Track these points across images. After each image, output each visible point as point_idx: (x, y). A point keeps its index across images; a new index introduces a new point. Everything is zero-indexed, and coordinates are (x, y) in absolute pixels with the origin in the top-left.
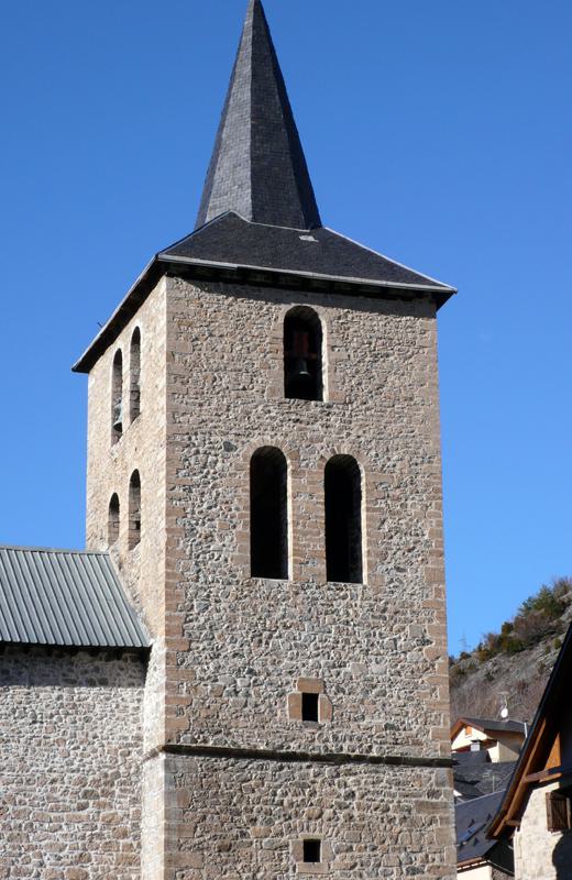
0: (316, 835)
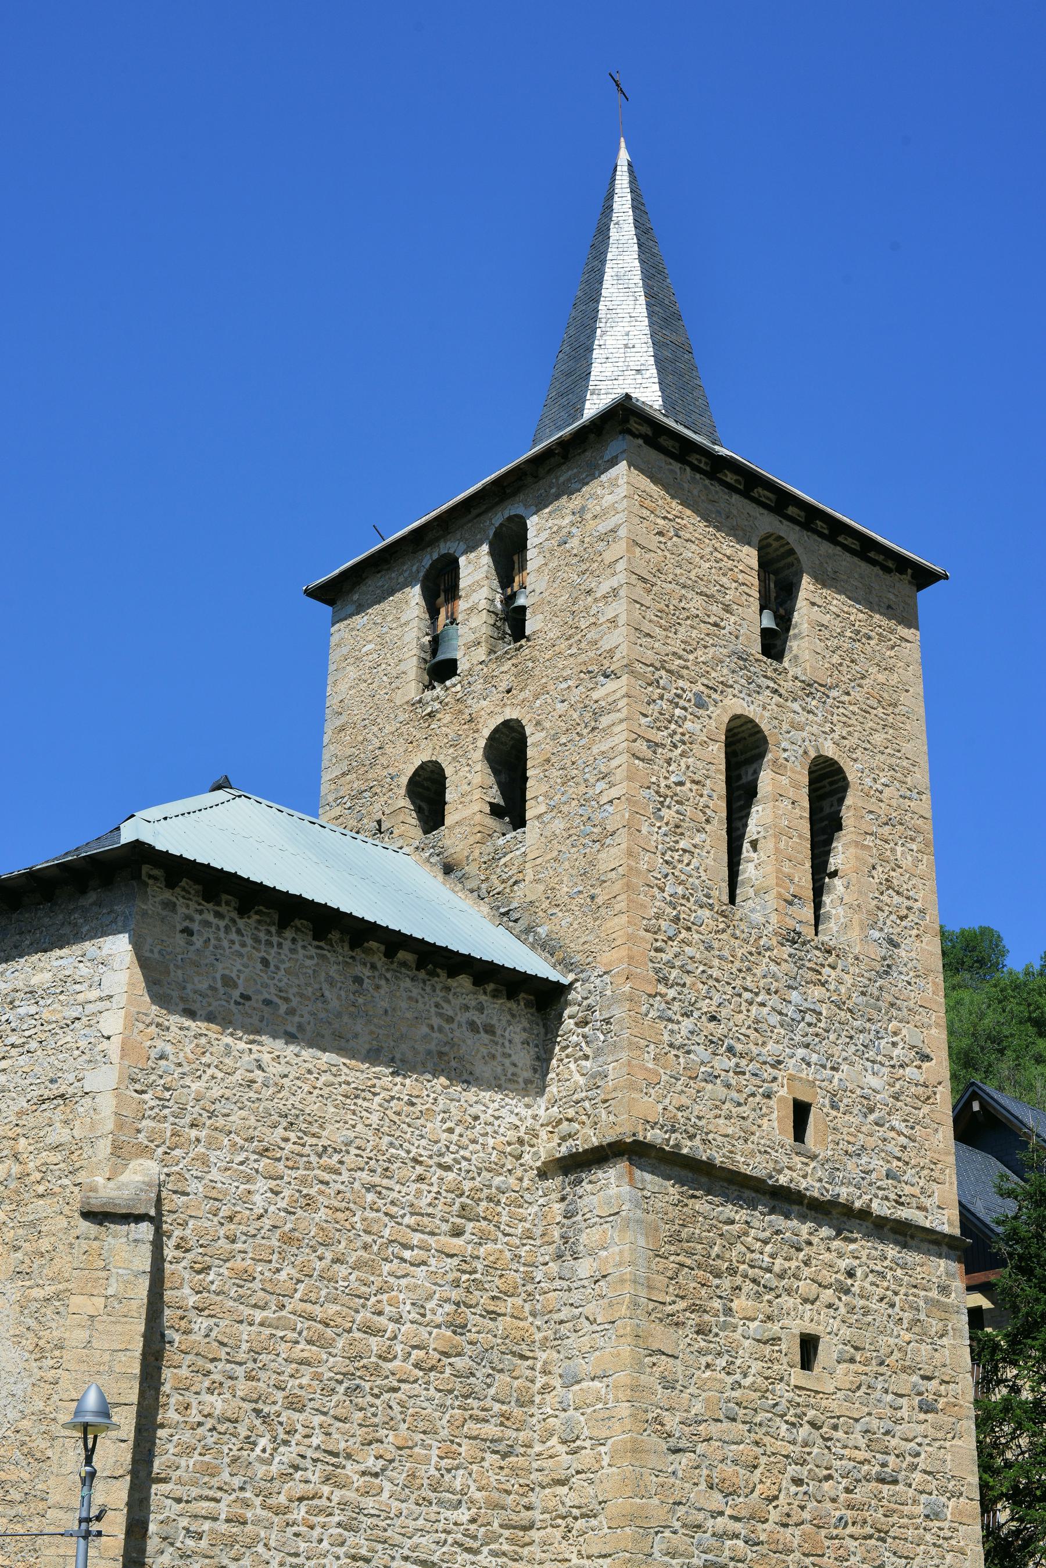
0: (811, 1329)
